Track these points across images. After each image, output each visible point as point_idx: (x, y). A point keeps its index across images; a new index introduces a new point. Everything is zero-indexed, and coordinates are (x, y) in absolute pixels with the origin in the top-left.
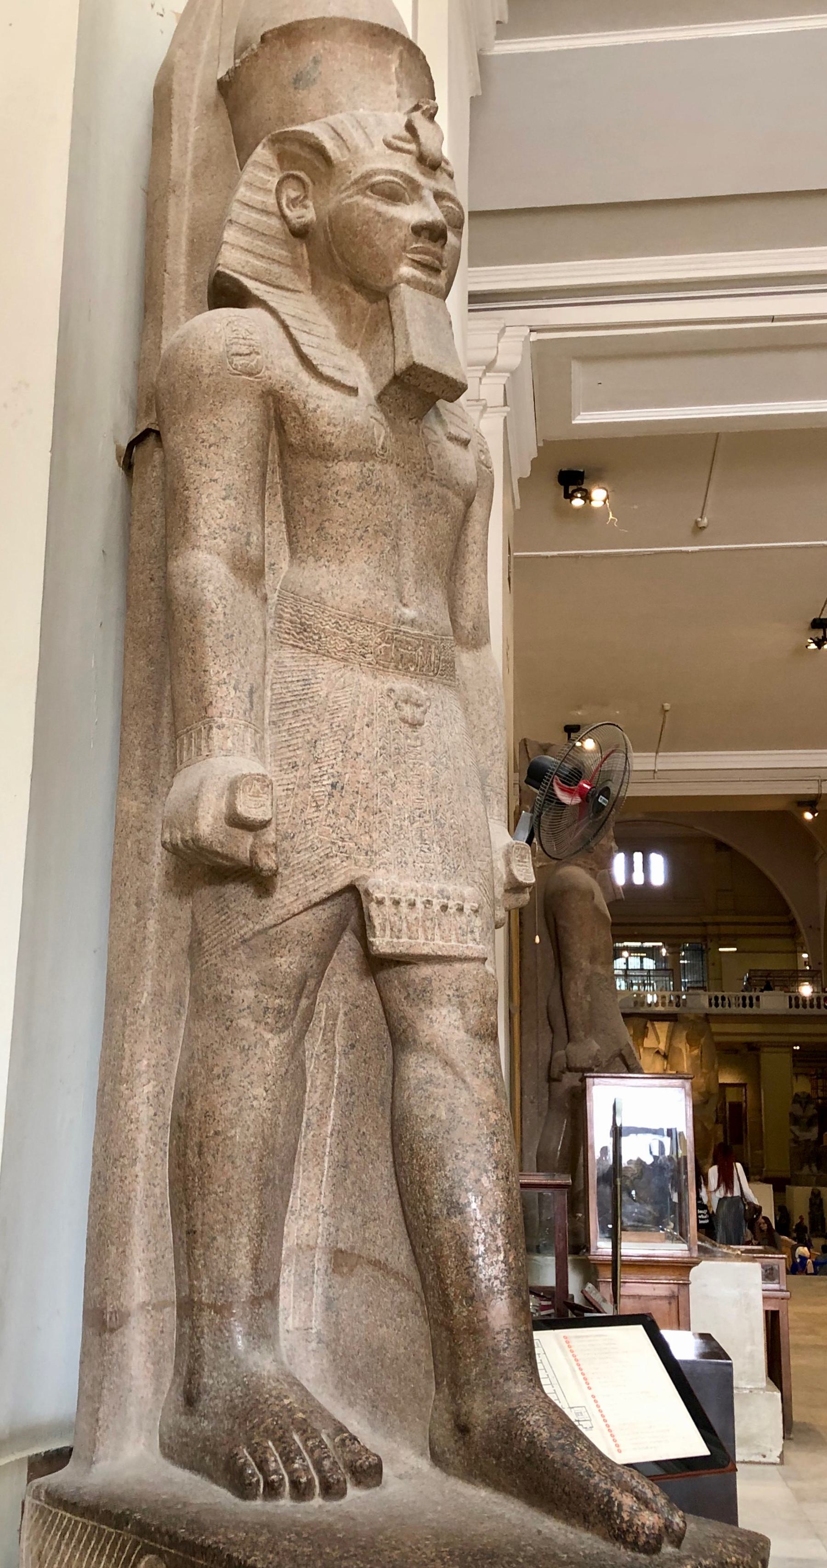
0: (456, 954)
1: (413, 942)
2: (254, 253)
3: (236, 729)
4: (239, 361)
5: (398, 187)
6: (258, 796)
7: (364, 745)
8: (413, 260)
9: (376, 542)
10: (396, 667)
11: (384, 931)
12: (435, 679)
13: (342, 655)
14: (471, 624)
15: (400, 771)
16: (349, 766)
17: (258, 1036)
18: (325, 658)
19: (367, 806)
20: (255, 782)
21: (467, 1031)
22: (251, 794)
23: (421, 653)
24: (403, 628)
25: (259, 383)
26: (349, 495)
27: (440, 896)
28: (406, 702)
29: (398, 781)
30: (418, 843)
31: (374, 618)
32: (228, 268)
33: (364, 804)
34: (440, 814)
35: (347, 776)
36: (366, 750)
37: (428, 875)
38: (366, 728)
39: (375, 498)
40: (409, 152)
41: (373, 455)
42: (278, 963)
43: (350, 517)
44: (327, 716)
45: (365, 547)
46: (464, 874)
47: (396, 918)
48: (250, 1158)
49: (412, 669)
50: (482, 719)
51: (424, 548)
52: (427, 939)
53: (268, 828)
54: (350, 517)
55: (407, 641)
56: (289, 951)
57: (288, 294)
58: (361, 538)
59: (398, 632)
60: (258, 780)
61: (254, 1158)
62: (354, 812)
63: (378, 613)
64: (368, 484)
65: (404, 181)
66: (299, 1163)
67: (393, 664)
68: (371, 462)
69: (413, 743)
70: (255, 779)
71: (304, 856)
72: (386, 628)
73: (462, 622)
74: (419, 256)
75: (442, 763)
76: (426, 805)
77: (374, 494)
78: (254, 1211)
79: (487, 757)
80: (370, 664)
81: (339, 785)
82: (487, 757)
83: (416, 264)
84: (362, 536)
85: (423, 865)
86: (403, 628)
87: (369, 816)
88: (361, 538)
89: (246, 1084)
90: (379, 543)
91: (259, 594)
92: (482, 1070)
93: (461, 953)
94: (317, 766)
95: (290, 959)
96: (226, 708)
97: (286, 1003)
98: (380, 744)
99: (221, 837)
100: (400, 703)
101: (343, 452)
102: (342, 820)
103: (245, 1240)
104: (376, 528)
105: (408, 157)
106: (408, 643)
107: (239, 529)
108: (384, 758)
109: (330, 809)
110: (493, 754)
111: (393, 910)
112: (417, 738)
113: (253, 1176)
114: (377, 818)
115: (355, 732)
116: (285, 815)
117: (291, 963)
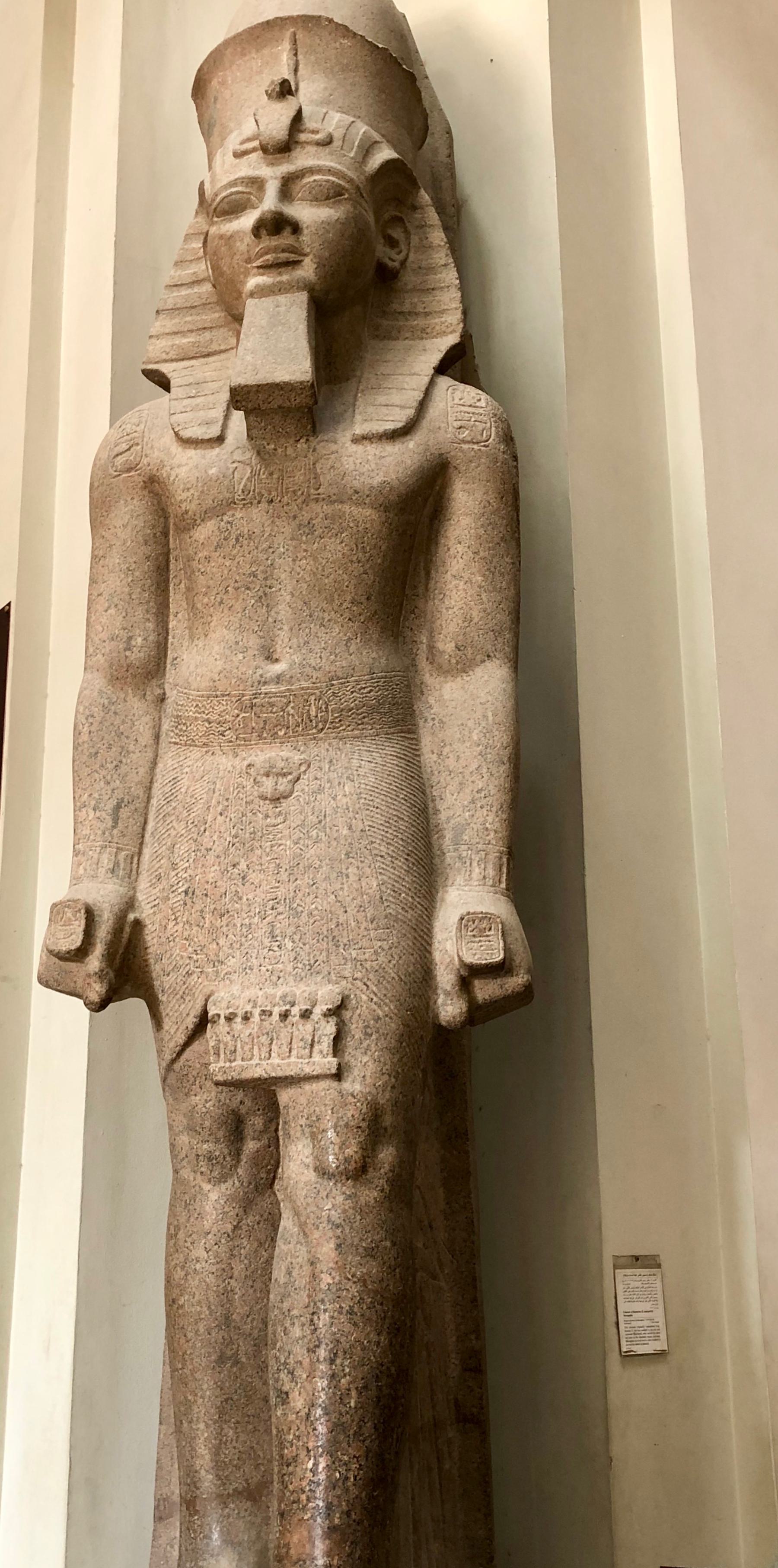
0: (292, 1073)
2: (181, 332)
3: (91, 853)
4: (120, 460)
5: (238, 196)
6: (69, 925)
7: (215, 838)
8: (258, 267)
9: (237, 600)
11: (219, 1055)
12: (321, 735)
14: (453, 645)
15: (254, 859)
16: (200, 866)
17: (197, 1188)
18: (192, 748)
19: (215, 909)
20: (66, 909)
21: (316, 1169)
22: (62, 923)
23: (292, 712)
24: (264, 689)
25: (139, 475)
26: (208, 559)
27: (281, 1003)
29: (251, 871)
30: (267, 942)
31: (229, 689)
32: (151, 363)
33: (212, 907)
34: (298, 901)
35: (197, 878)
36: (217, 843)
37: (274, 978)
38: (219, 817)
39: (235, 552)
40: (254, 150)
41: (231, 503)
42: (193, 1103)
44: (185, 814)
45: (226, 611)
48: (198, 1330)
49: (281, 733)
50: (461, 761)
51: (305, 586)
52: (260, 1059)
53: (91, 957)
54: (211, 582)
55: (269, 703)
56: (201, 1088)
57: (223, 356)
58: (221, 603)
59: (256, 695)
60: (69, 907)
61: (202, 1330)
62: (204, 918)
63: (233, 681)
65: (247, 186)
67: (255, 735)
68: (230, 513)
70: (65, 907)
72: (243, 695)
73: (440, 646)
74: (261, 260)
76: (280, 893)
77: (234, 547)
78: (208, 1393)
79: (464, 807)
80: (231, 742)
81: (191, 890)
82: (464, 807)
83: (261, 270)
84: (222, 599)
85: (270, 968)
86: (264, 689)
87: (216, 920)
88: (221, 603)
89: (188, 1244)
90: (240, 601)
91: (148, 698)
92: (325, 1219)
93: (299, 1072)
94: (174, 873)
95: (205, 1097)
96: (84, 832)
98: (233, 832)
100: (259, 778)
101: (198, 515)
102: (195, 928)
103: (202, 1426)
104: (236, 585)
105: (254, 156)
106: (272, 705)
107: (117, 636)
108: (237, 849)
109: (185, 919)
112: (280, 813)
113: (203, 1351)
115: (207, 826)
116: (154, 935)
117: (206, 1101)
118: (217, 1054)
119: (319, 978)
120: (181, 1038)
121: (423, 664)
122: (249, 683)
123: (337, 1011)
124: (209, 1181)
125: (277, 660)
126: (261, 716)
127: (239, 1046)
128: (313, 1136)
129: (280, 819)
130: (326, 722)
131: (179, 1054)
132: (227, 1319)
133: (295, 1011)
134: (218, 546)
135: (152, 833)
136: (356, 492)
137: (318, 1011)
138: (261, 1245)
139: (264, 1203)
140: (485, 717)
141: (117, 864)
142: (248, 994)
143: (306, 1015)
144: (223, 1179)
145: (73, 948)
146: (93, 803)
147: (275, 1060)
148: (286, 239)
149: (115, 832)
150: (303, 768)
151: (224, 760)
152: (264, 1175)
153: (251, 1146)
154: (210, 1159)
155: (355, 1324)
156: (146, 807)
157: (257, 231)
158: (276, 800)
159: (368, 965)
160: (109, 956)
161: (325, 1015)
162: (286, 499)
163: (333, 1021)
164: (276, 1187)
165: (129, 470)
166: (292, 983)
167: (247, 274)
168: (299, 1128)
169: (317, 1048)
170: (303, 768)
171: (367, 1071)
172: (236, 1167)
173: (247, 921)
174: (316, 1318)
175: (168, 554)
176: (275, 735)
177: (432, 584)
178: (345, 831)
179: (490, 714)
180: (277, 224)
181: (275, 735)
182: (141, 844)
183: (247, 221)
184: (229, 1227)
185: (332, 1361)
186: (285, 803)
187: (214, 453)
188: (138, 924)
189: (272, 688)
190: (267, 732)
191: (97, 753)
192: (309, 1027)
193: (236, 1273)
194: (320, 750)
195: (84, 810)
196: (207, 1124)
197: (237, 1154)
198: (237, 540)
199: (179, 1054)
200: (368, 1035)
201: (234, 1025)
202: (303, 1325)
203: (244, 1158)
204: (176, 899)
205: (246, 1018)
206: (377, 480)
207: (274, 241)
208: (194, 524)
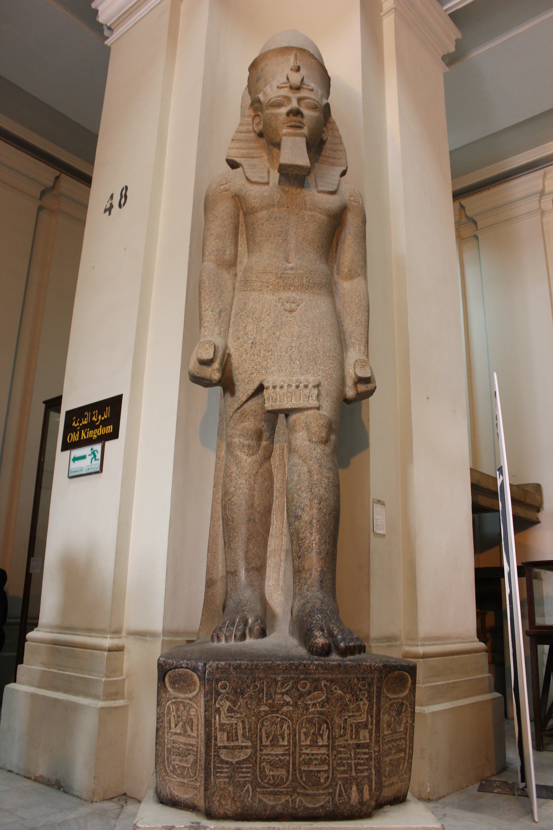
1: (281, 403)
4: (222, 187)
10: (284, 289)
13: (259, 289)
24: (286, 272)
26: (263, 224)
28: (287, 303)
37: (292, 374)
41: (273, 206)
43: (263, 233)
46: (312, 372)
47: (274, 394)
49: (292, 288)
54: (263, 233)
59: (283, 274)
64: (271, 218)
66: (274, 514)
69: (290, 319)
71: (243, 375)
75: (305, 326)
86: (286, 272)
97: (253, 443)
99: (197, 370)
105: (286, 89)
106: (289, 278)
110: (356, 323)
111: (273, 391)
114: (270, 353)
118: (269, 400)
119: (310, 375)
120: (244, 399)
121: (335, 275)
122: (280, 269)
123: (317, 386)
124: (247, 455)
125: (290, 263)
126: (284, 282)
127: (278, 397)
128: (308, 429)
129: (293, 319)
130: (309, 286)
131: (242, 406)
132: (252, 505)
133: (302, 385)
134: (267, 220)
135: (234, 323)
136: (320, 209)
137: (310, 386)
138: (265, 479)
139: (266, 465)
140: (360, 295)
141: (220, 332)
142: (281, 379)
143: (306, 387)
144: (253, 454)
145: (210, 358)
146: (211, 309)
147: (294, 402)
148: (298, 118)
149: (220, 320)
150: (300, 301)
151: (268, 296)
152: (267, 454)
153: (264, 443)
154: (249, 446)
155: (327, 492)
156: (230, 313)
157: (288, 114)
158: (291, 311)
159: (327, 372)
160: (221, 364)
161: (314, 387)
162: (293, 207)
163: (316, 389)
164: (271, 459)
165: (226, 191)
166: (299, 376)
167: (283, 128)
168: (301, 427)
169: (310, 398)
170: (300, 301)
171: (327, 409)
172: (258, 450)
173: (280, 354)
174: (312, 490)
175: (239, 223)
176: (289, 289)
177: (339, 248)
178: (318, 325)
179: (362, 295)
180: (297, 113)
181: (289, 289)
182: (229, 326)
183: (284, 110)
184: (254, 472)
185: (320, 504)
186: (294, 314)
187: (266, 187)
188: (229, 355)
189: (289, 272)
190: (286, 287)
191: (212, 291)
192: (308, 391)
193: (256, 490)
194: (305, 297)
195: (207, 312)
196: (250, 433)
197: (259, 446)
198: (275, 218)
199: (242, 406)
200: (328, 396)
201: (276, 390)
202: (307, 492)
203: (261, 447)
204: (247, 346)
205: (282, 387)
206: (328, 206)
207: (294, 118)
208: (257, 211)
